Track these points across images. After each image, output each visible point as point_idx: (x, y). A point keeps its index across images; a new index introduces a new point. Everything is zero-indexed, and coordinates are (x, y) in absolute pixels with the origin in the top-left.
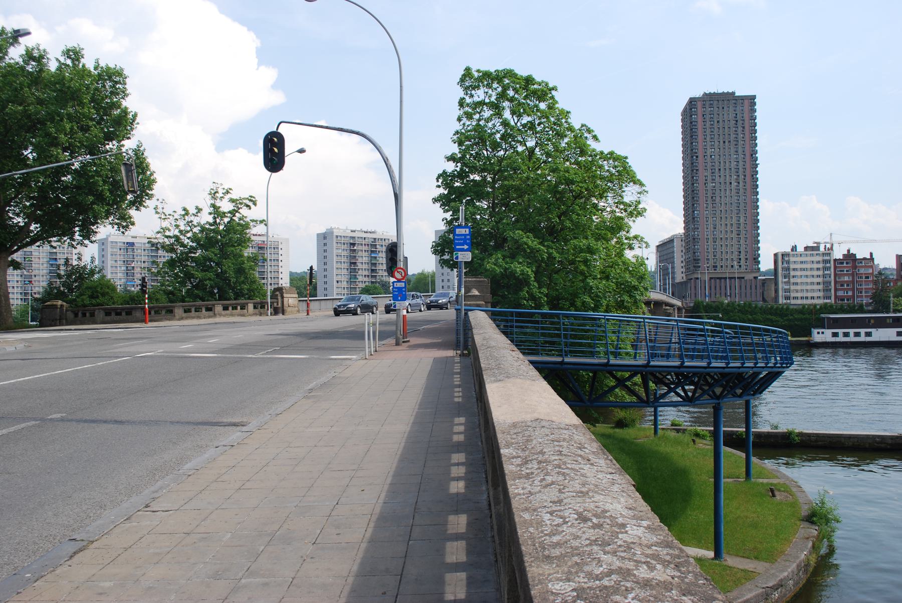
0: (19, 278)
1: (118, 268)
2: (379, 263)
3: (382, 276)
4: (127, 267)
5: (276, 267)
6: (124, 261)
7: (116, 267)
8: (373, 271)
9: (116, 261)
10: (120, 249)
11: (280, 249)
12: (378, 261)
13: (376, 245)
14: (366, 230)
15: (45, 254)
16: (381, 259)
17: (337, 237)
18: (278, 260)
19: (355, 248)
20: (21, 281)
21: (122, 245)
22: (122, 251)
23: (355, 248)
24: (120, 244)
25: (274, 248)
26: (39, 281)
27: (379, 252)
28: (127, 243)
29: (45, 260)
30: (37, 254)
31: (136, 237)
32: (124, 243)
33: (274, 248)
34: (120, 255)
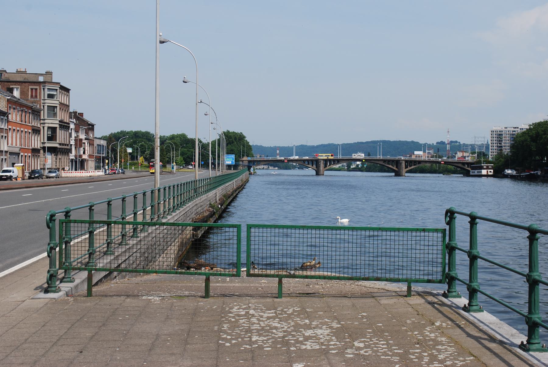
0: (496, 148)
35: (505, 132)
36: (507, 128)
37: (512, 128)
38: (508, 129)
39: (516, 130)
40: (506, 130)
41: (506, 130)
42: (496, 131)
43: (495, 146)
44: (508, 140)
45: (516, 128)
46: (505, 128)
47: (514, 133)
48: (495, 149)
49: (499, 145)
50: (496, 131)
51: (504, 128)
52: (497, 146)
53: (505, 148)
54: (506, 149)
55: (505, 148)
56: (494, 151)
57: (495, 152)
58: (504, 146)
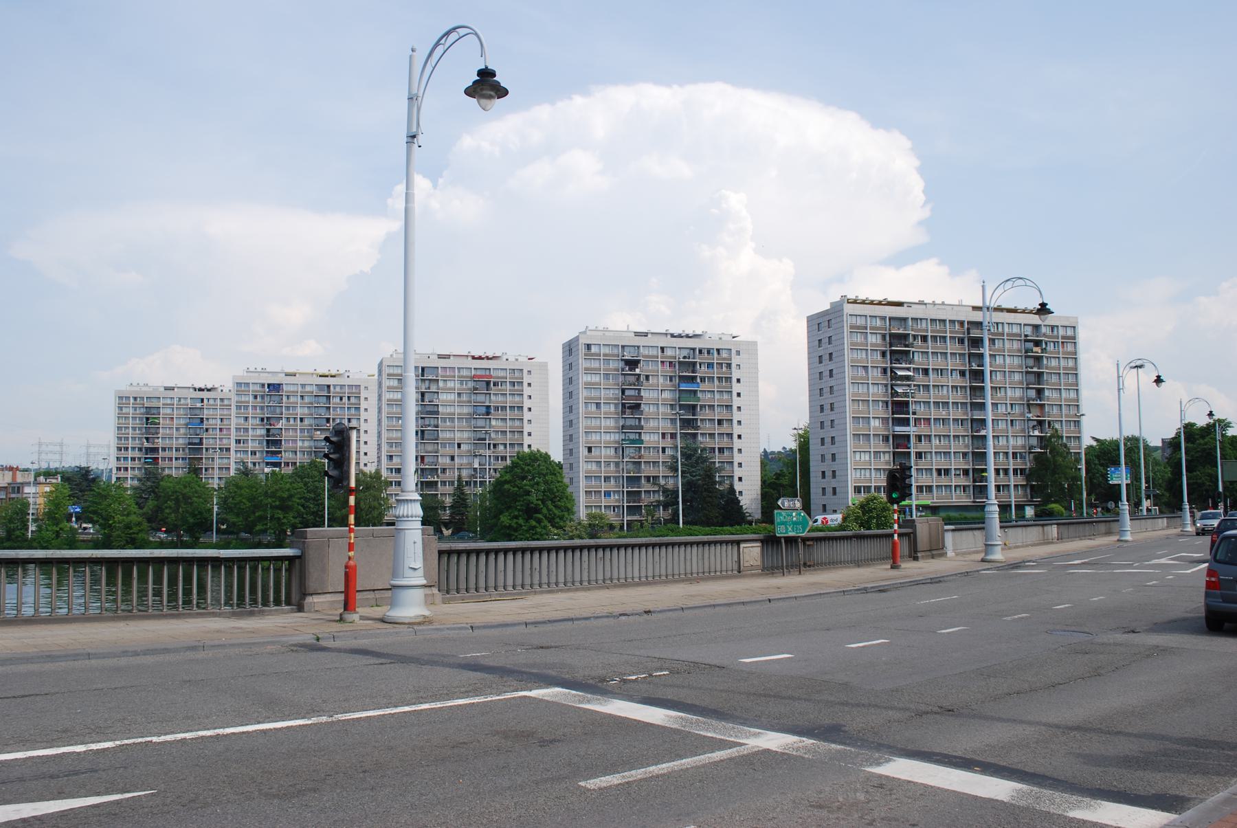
0: (137, 454)
1: (250, 432)
2: (702, 407)
3: (712, 435)
4: (268, 430)
5: (517, 423)
6: (262, 419)
7: (246, 430)
8: (686, 423)
9: (246, 418)
10: (256, 397)
11: (525, 384)
12: (699, 400)
13: (694, 364)
14: (676, 332)
15: (182, 412)
16: (709, 395)
17: (589, 346)
18: (521, 408)
19: (638, 371)
20: (139, 459)
21: (258, 388)
22: (259, 399)
23: (638, 371)
24: (258, 388)
25: (513, 384)
26: (171, 459)
27: (703, 379)
28: (269, 385)
29: (182, 422)
30: (169, 411)
31: (295, 375)
32: (263, 385)
33: (513, 384)
34: (254, 407)
35: (169, 401)
36: (173, 389)
37: (191, 390)
38: (176, 394)
39: (205, 395)
40: (170, 394)
41: (170, 394)
42: (135, 399)
43: (133, 449)
44: (177, 429)
45: (201, 390)
46: (166, 389)
47: (199, 405)
48: (133, 459)
49: (146, 444)
50: (135, 399)
51: (163, 389)
52: (140, 449)
53: (167, 454)
54: (171, 459)
55: (167, 454)
56: (129, 464)
57: (133, 469)
58: (164, 449)
